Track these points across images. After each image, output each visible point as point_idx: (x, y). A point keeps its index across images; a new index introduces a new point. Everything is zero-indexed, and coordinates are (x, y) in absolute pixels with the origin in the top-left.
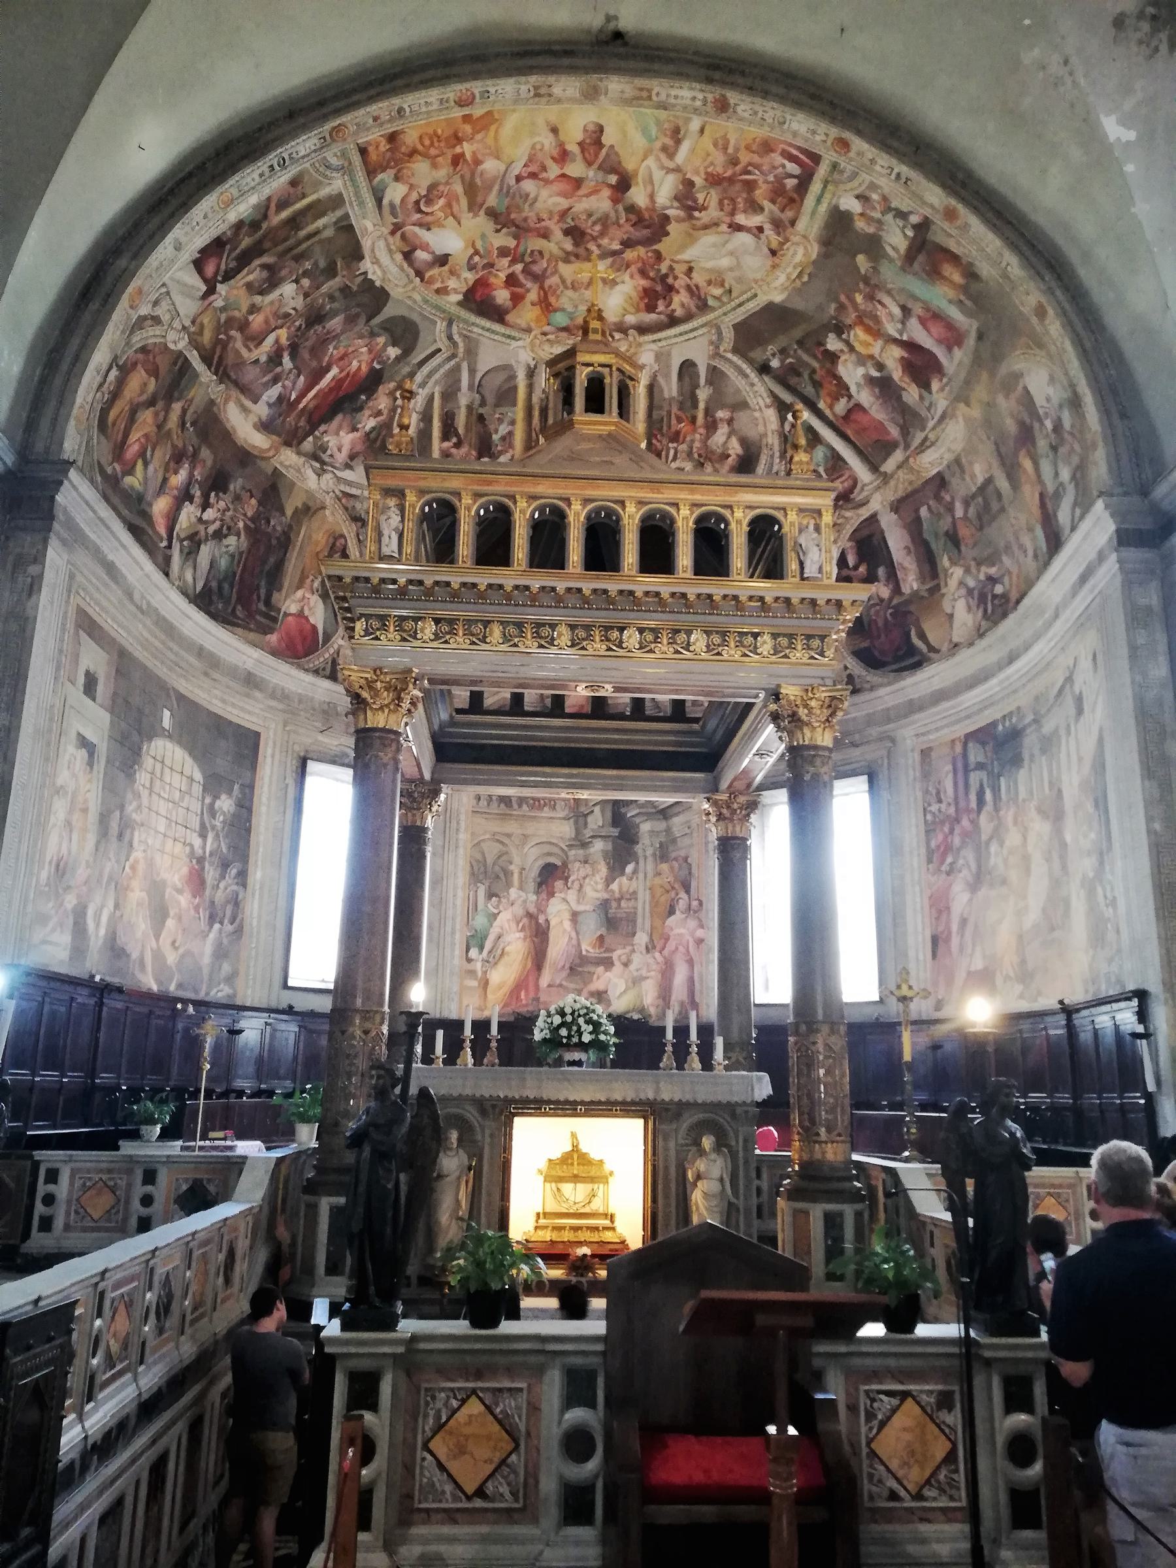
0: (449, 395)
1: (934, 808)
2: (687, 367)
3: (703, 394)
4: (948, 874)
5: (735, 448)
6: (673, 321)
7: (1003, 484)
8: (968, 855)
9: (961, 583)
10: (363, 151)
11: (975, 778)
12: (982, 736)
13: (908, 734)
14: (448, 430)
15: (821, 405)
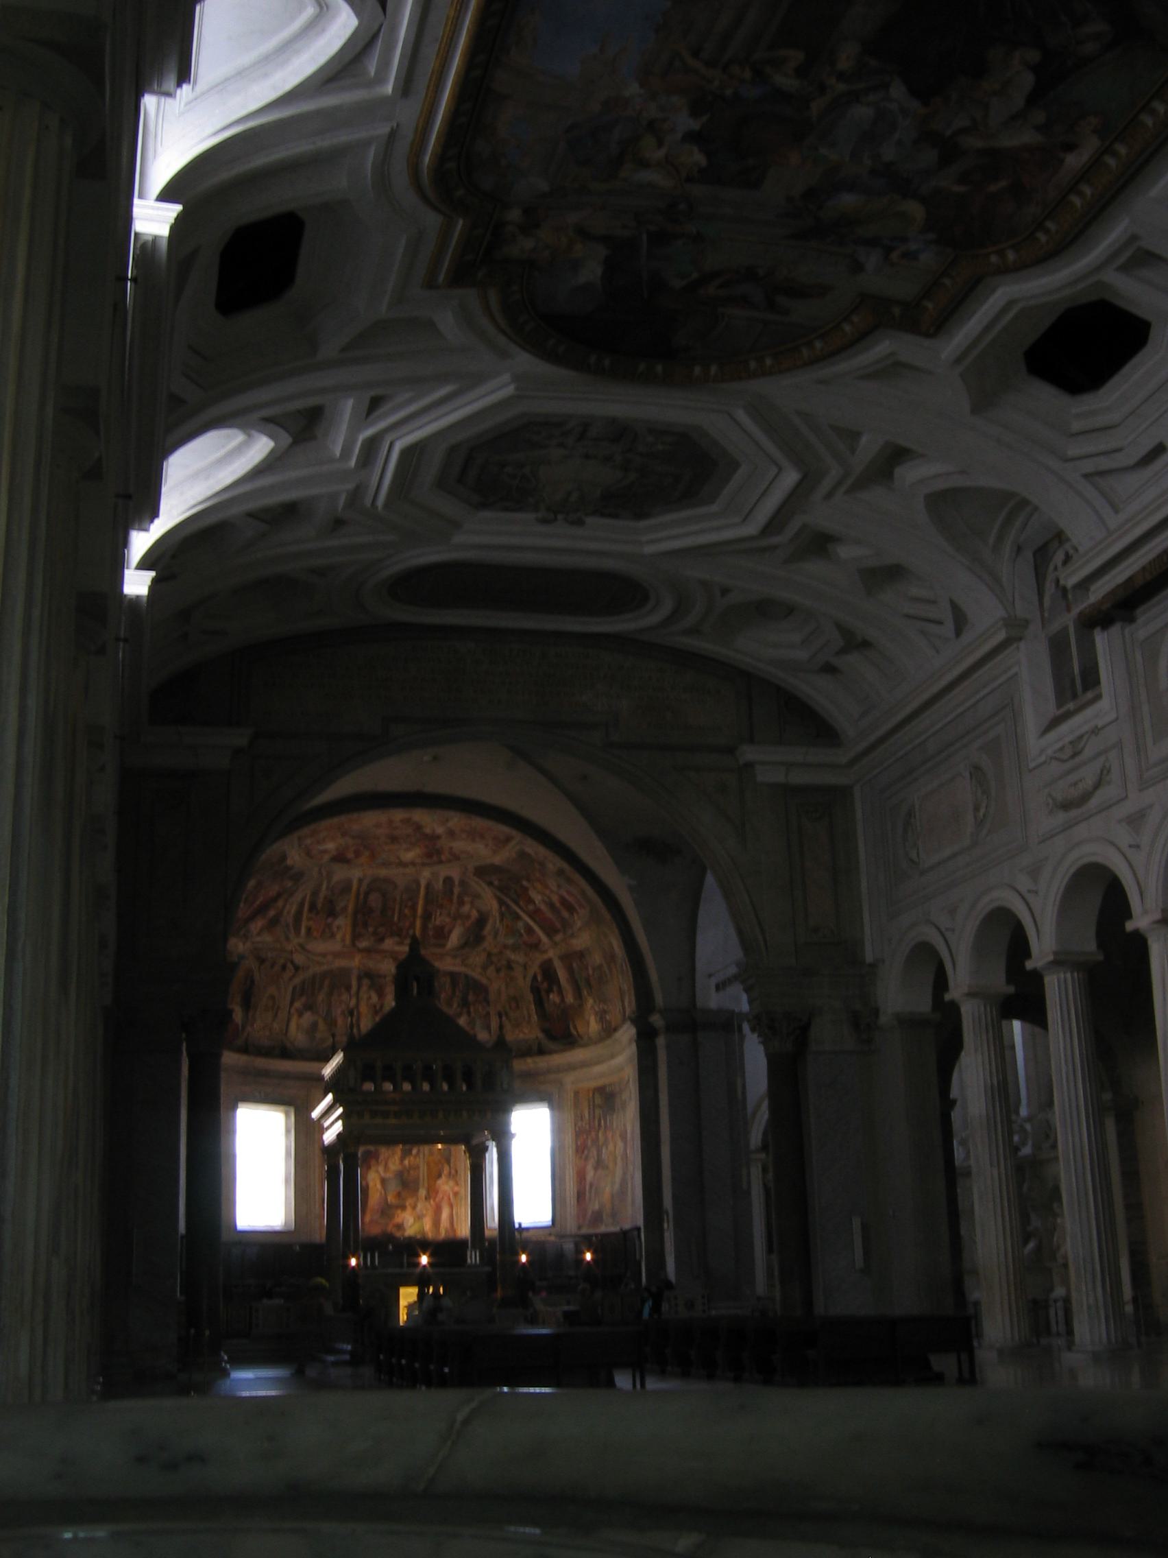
0: (315, 893)
1: (580, 1124)
2: (448, 881)
3: (456, 890)
4: (587, 1159)
5: (475, 914)
6: (441, 862)
7: (605, 968)
8: (594, 1152)
9: (592, 1007)
10: (299, 839)
11: (598, 1112)
12: (600, 1090)
13: (569, 1079)
14: (313, 907)
15: (521, 903)
